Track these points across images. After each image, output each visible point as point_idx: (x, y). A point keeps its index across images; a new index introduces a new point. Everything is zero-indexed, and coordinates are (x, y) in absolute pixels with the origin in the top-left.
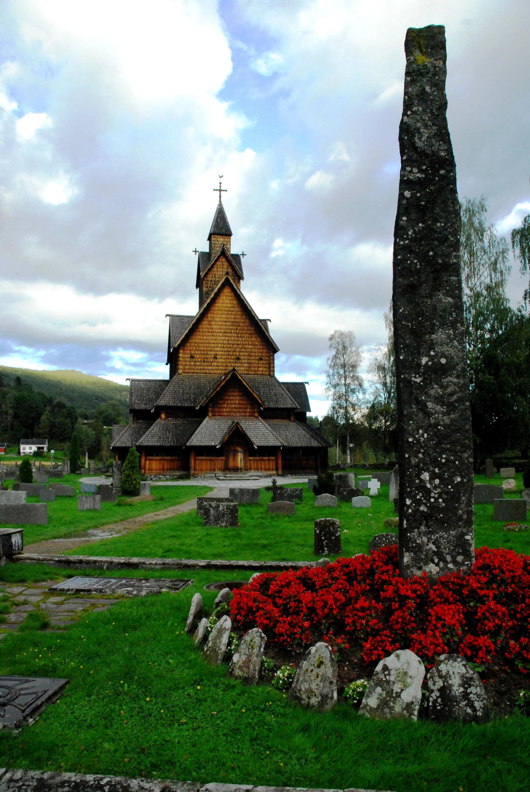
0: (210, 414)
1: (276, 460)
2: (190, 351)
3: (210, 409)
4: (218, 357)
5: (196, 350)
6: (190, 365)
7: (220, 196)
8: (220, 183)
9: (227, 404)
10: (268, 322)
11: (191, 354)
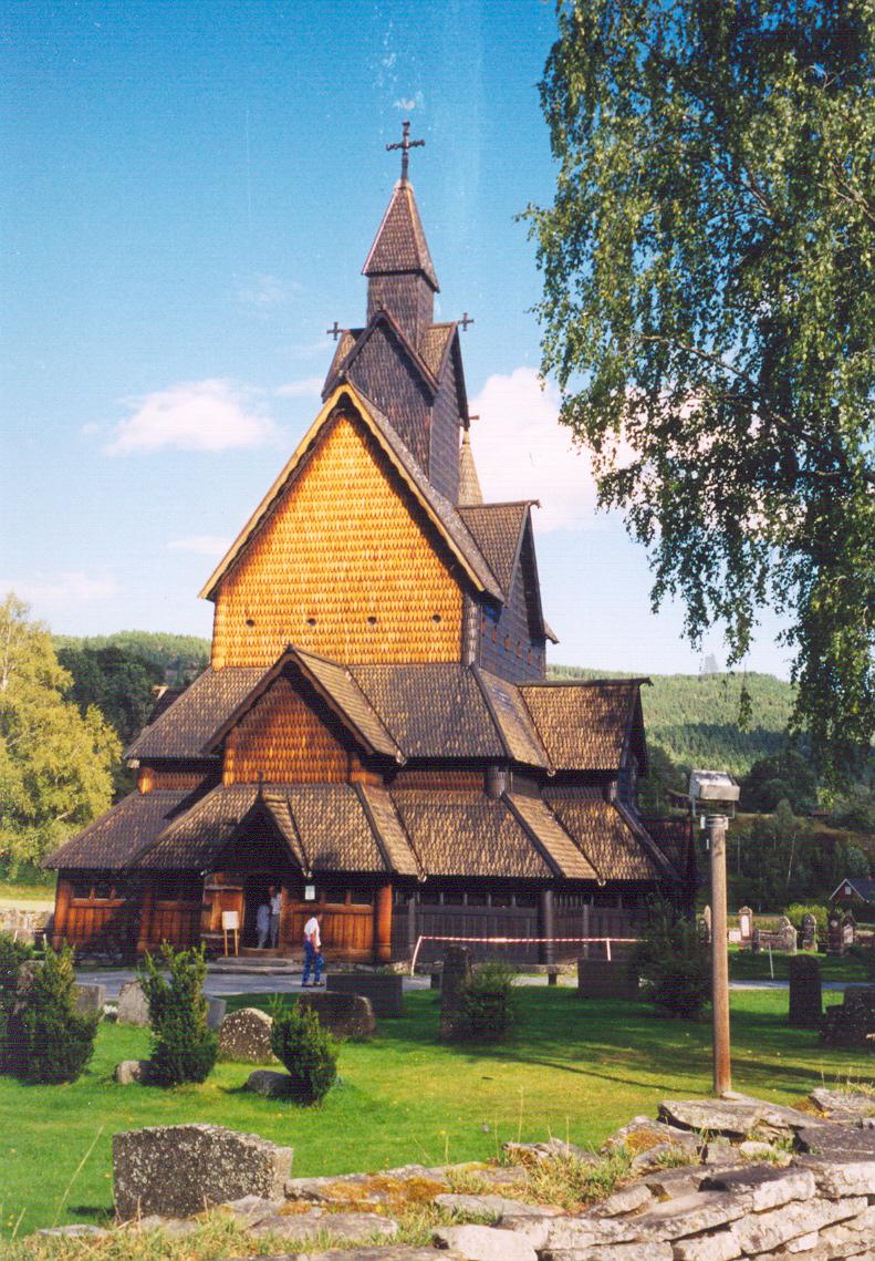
0: (228, 778)
1: (376, 916)
2: (247, 605)
3: (230, 764)
4: (318, 617)
5: (262, 602)
6: (243, 644)
7: (405, 163)
8: (407, 124)
9: (277, 747)
10: (533, 508)
11: (247, 613)
